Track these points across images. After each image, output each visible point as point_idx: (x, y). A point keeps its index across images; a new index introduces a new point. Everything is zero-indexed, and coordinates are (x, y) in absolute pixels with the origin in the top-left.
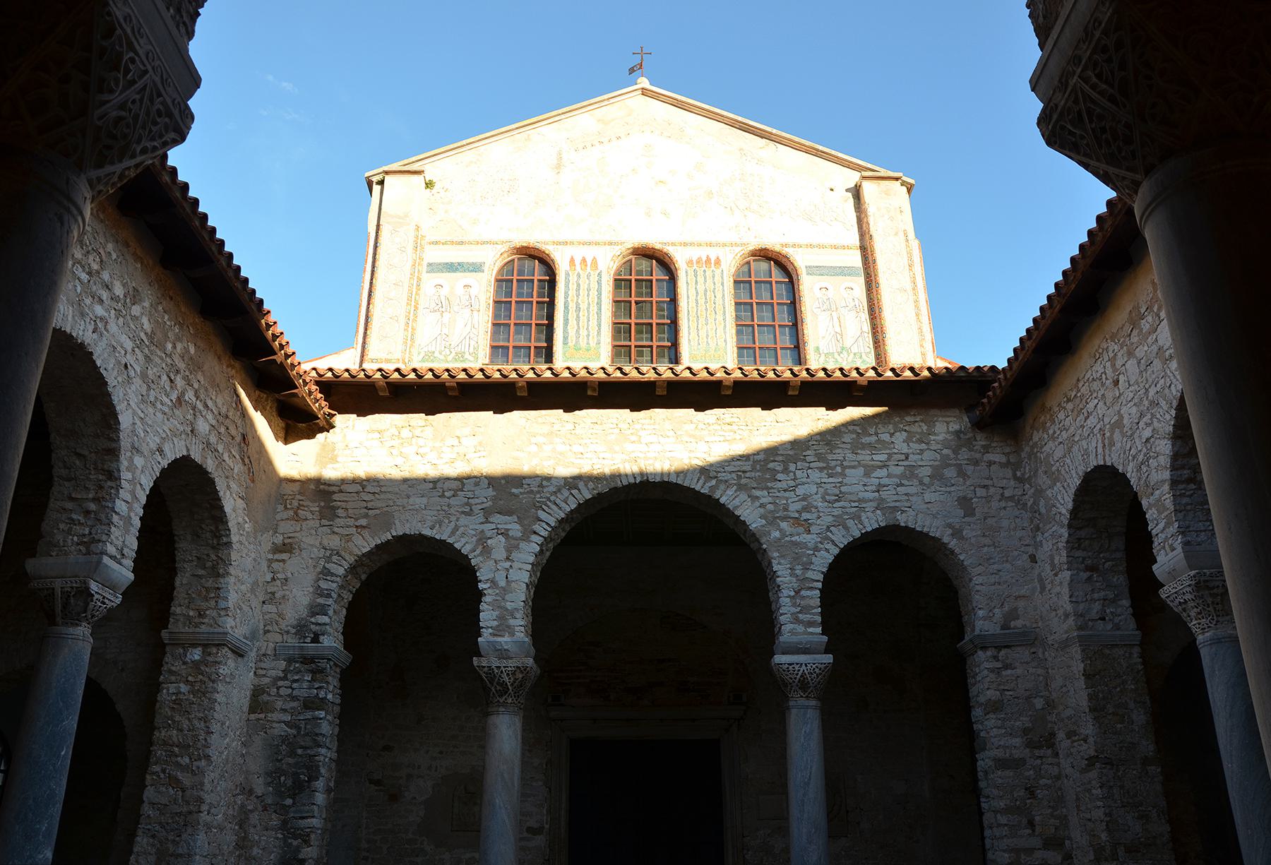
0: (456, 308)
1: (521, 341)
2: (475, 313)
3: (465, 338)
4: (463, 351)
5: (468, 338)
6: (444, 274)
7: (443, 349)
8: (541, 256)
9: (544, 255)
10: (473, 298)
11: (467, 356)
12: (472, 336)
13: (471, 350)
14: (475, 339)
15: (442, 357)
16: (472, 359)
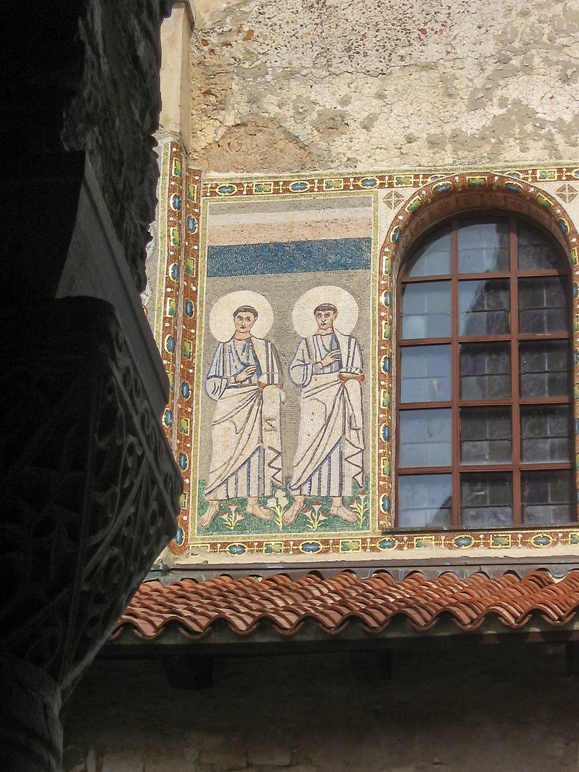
0: (297, 375)
1: (480, 457)
2: (353, 386)
3: (328, 457)
4: (324, 493)
5: (335, 456)
6: (258, 279)
7: (268, 493)
8: (525, 211)
9: (534, 208)
10: (343, 341)
11: (337, 508)
12: (348, 450)
13: (348, 492)
14: (357, 460)
15: (262, 513)
16: (345, 513)
